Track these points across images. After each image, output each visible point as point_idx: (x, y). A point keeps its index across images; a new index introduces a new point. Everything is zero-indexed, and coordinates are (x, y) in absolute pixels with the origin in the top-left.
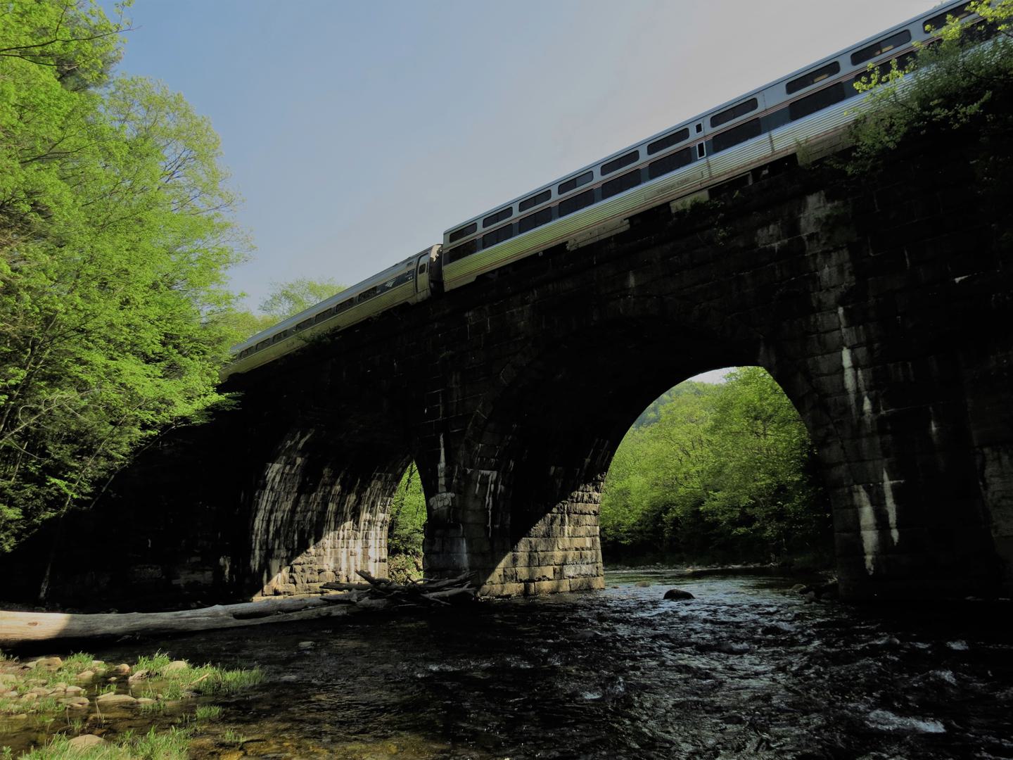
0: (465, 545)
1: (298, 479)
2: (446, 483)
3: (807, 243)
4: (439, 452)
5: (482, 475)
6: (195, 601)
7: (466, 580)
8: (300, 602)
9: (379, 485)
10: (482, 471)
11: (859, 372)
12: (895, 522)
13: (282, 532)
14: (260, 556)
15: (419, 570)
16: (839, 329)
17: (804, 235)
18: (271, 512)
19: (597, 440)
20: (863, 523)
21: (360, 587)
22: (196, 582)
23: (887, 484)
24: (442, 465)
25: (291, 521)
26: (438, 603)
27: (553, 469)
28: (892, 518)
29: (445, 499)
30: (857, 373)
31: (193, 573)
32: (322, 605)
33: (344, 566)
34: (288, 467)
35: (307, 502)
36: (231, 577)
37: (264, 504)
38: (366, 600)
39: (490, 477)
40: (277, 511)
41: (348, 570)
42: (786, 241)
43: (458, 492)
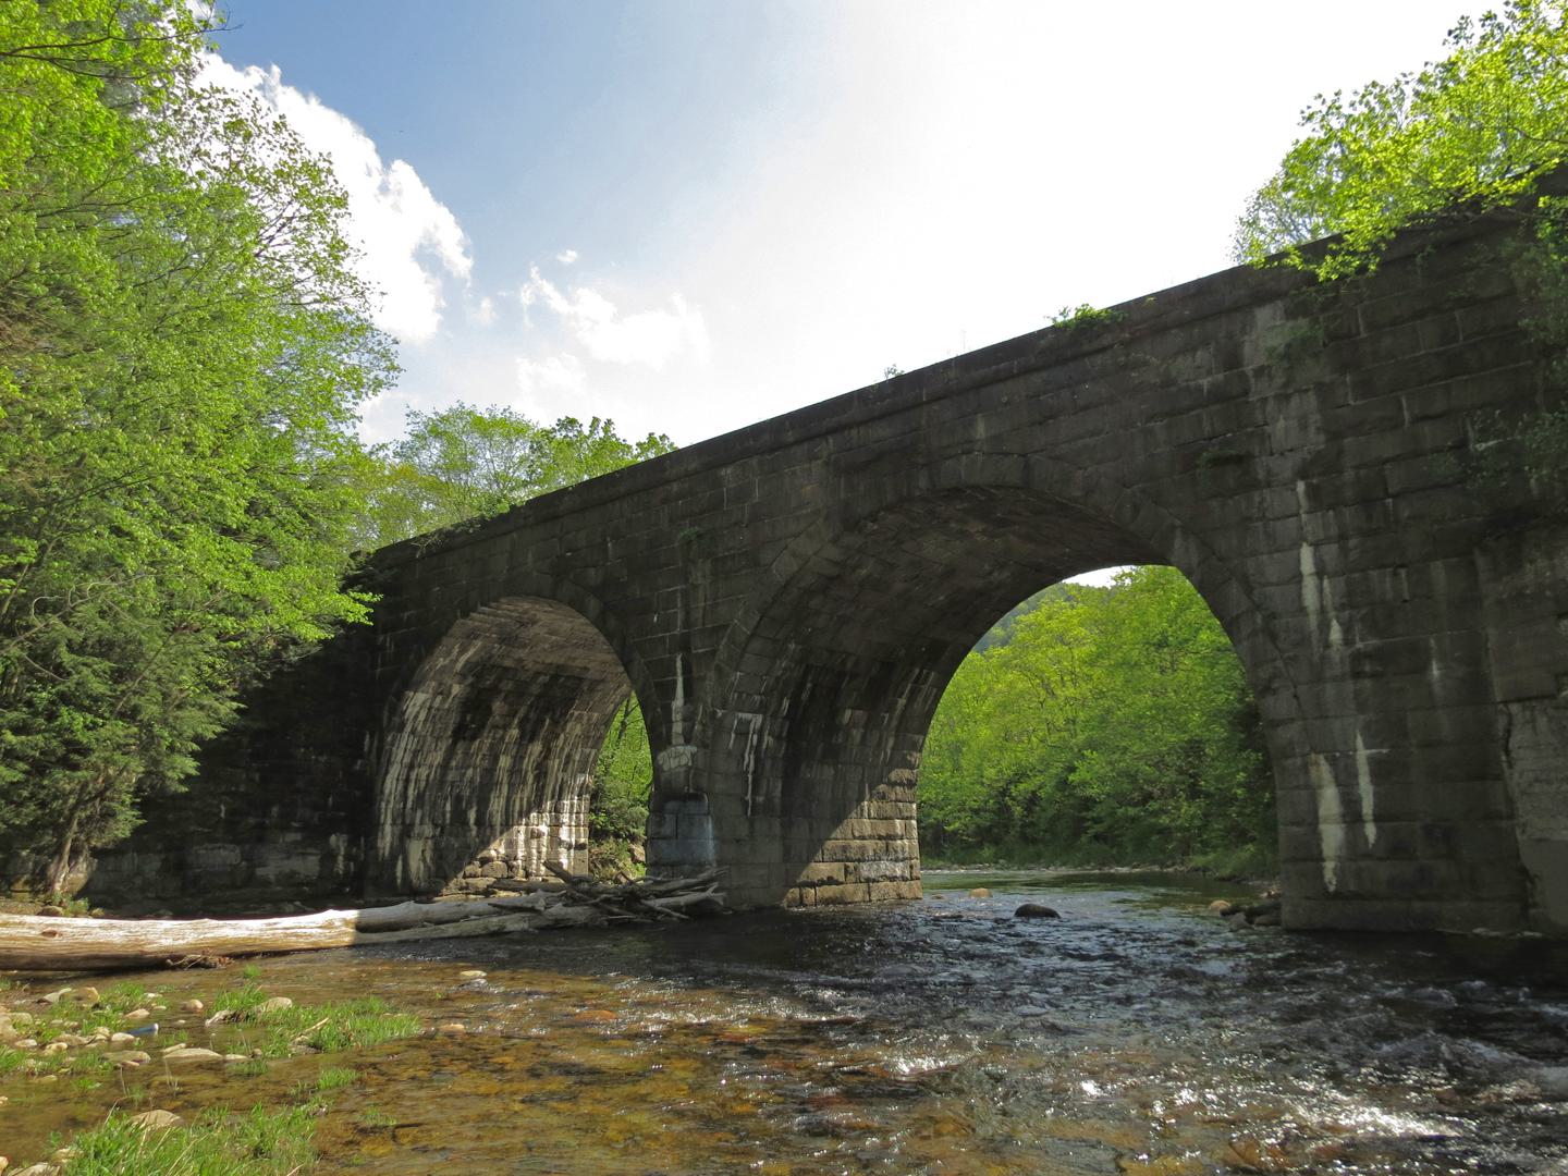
0: (710, 826)
1: (453, 720)
2: (684, 730)
3: (1252, 381)
5: (740, 721)
6: (291, 901)
7: (712, 880)
8: (456, 909)
9: (578, 730)
11: (1326, 582)
12: (1370, 812)
13: (427, 798)
14: (393, 834)
15: (635, 861)
16: (1297, 515)
17: (1249, 369)
18: (411, 767)
19: (917, 671)
20: (1322, 812)
21: (547, 888)
22: (293, 873)
23: (1362, 754)
24: (678, 702)
25: (442, 782)
26: (668, 915)
27: (848, 713)
28: (1367, 807)
29: (680, 756)
30: (1321, 583)
31: (288, 858)
32: (490, 914)
33: (521, 853)
34: (439, 698)
35: (466, 754)
36: (347, 867)
37: (401, 753)
38: (558, 909)
39: (752, 725)
40: (419, 766)
41: (528, 858)
42: (1221, 377)
43: (703, 745)
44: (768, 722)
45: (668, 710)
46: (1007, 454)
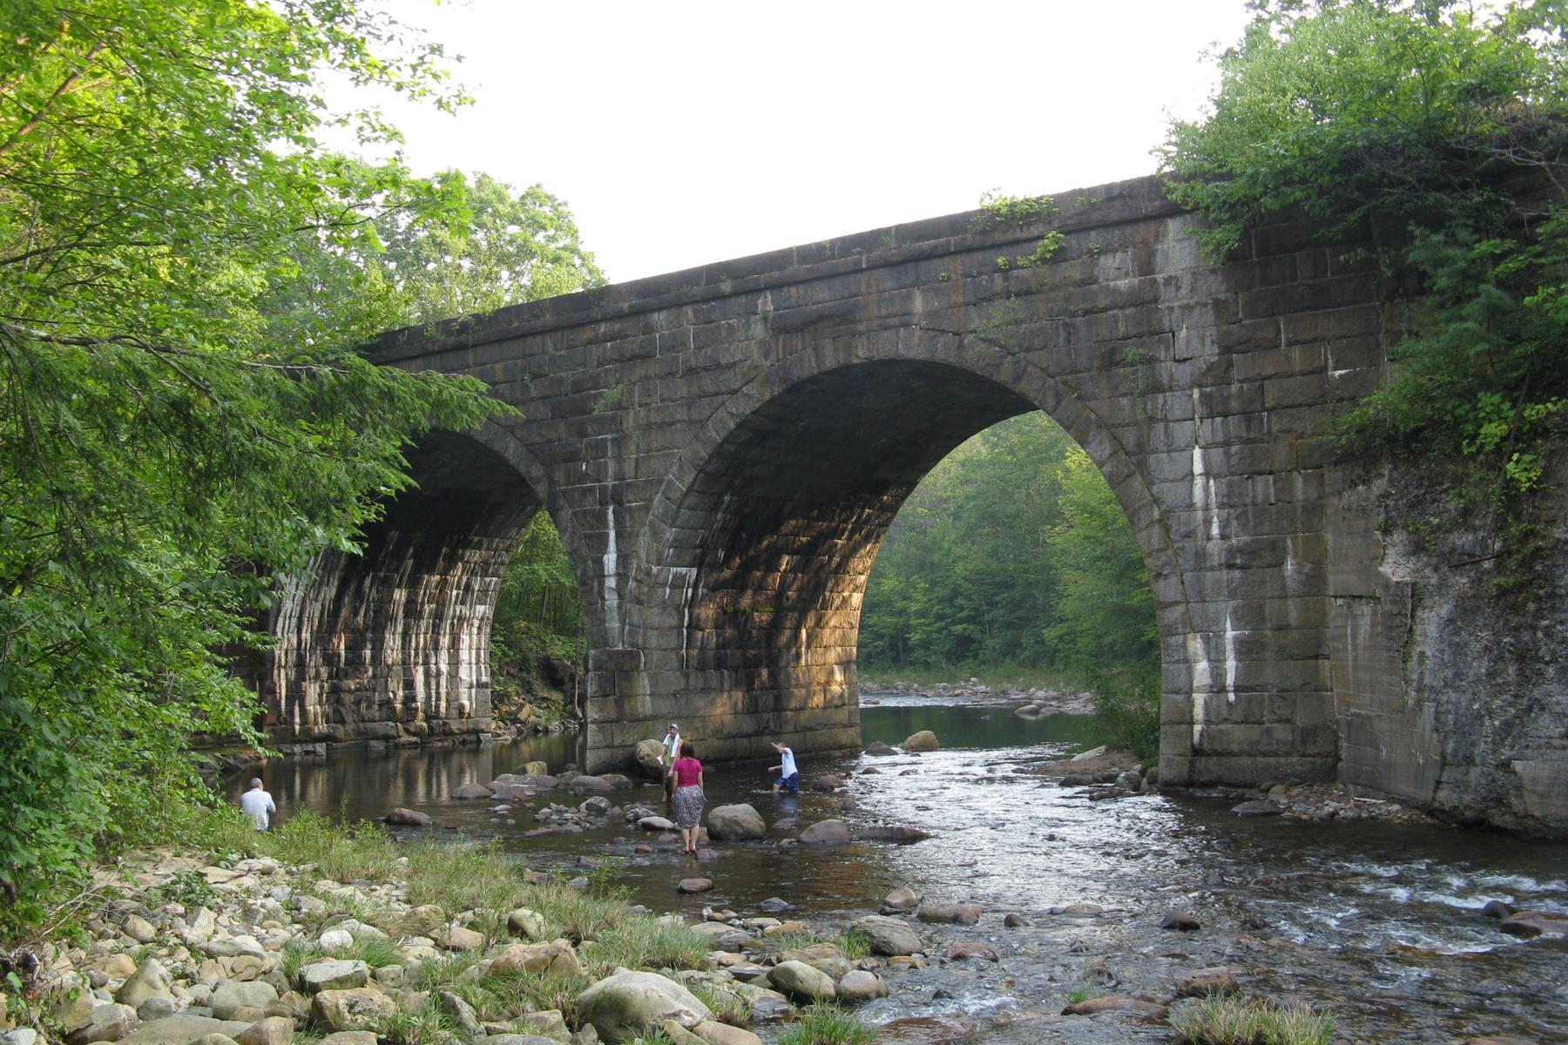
3: (1162, 289)
4: (607, 535)
11: (1212, 482)
16: (1193, 419)
30: (1208, 482)
42: (1136, 281)
45: (600, 563)
46: (943, 331)
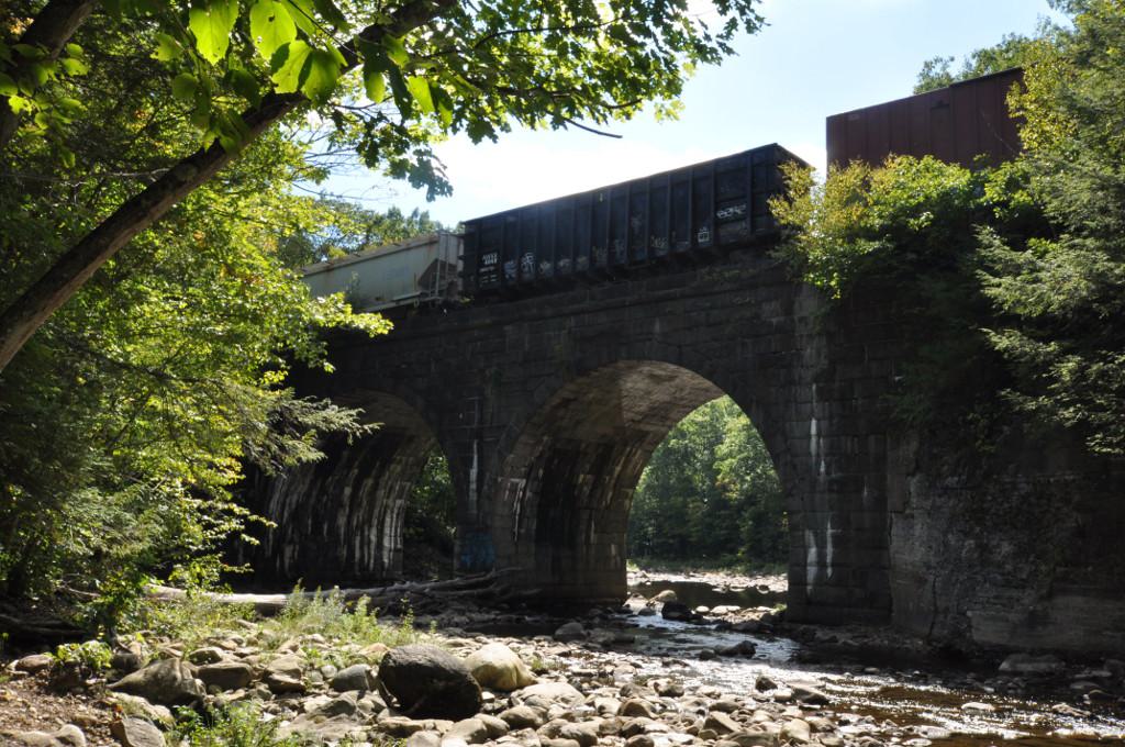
4: (472, 458)
5: (512, 484)
10: (513, 480)
19: (628, 449)
24: (474, 472)
27: (582, 476)
44: (530, 484)
45: (467, 474)
